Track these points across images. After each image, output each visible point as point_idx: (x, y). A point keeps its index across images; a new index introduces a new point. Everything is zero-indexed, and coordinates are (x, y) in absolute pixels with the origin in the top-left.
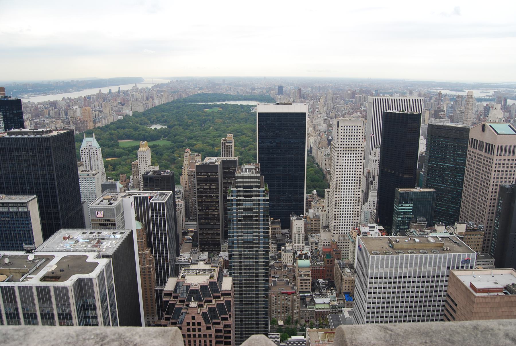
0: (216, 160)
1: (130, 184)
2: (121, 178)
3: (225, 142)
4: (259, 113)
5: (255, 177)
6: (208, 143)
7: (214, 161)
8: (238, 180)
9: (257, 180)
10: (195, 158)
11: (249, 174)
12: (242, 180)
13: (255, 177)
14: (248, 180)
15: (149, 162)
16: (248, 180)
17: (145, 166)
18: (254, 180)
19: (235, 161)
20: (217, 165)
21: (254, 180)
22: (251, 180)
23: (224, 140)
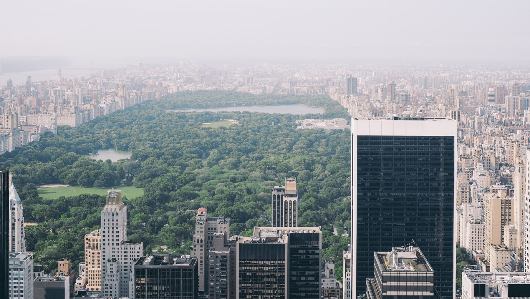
0: (281, 234)
1: (78, 281)
2: (60, 268)
3: (280, 193)
4: (360, 138)
5: (423, 279)
6: (222, 192)
7: (274, 235)
8: (389, 284)
9: (428, 284)
10: (219, 226)
11: (410, 270)
12: (396, 284)
13: (423, 279)
14: (408, 284)
15: (123, 236)
16: (408, 284)
17: (115, 242)
18: (421, 284)
19: (315, 236)
20: (283, 245)
21: (421, 284)
22: (416, 284)
23: (278, 190)
